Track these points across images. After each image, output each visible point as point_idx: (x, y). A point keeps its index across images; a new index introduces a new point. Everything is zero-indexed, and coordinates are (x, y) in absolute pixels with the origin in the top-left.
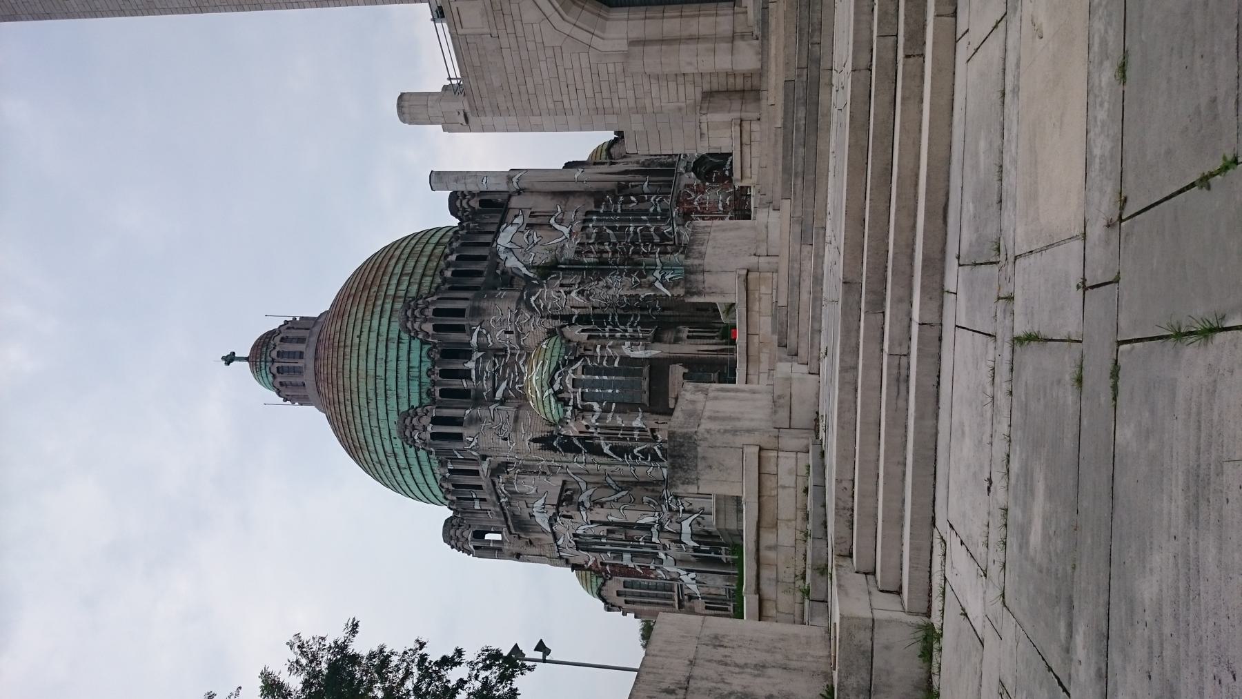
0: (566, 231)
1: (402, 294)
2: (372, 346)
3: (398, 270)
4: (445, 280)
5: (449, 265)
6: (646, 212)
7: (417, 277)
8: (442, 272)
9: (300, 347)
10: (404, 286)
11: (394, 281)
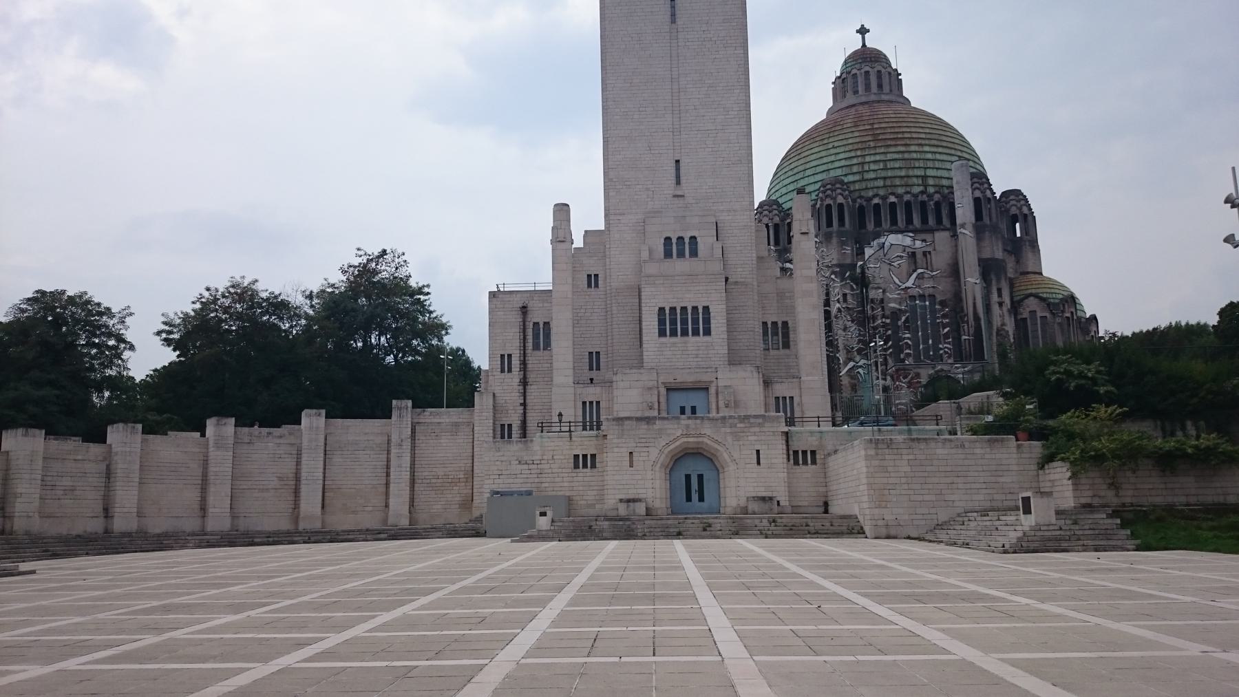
0: (910, 284)
1: (866, 168)
2: (825, 160)
3: (889, 156)
4: (884, 198)
5: (898, 196)
6: (936, 343)
7: (883, 174)
8: (876, 195)
9: (861, 89)
10: (873, 167)
11: (878, 157)
